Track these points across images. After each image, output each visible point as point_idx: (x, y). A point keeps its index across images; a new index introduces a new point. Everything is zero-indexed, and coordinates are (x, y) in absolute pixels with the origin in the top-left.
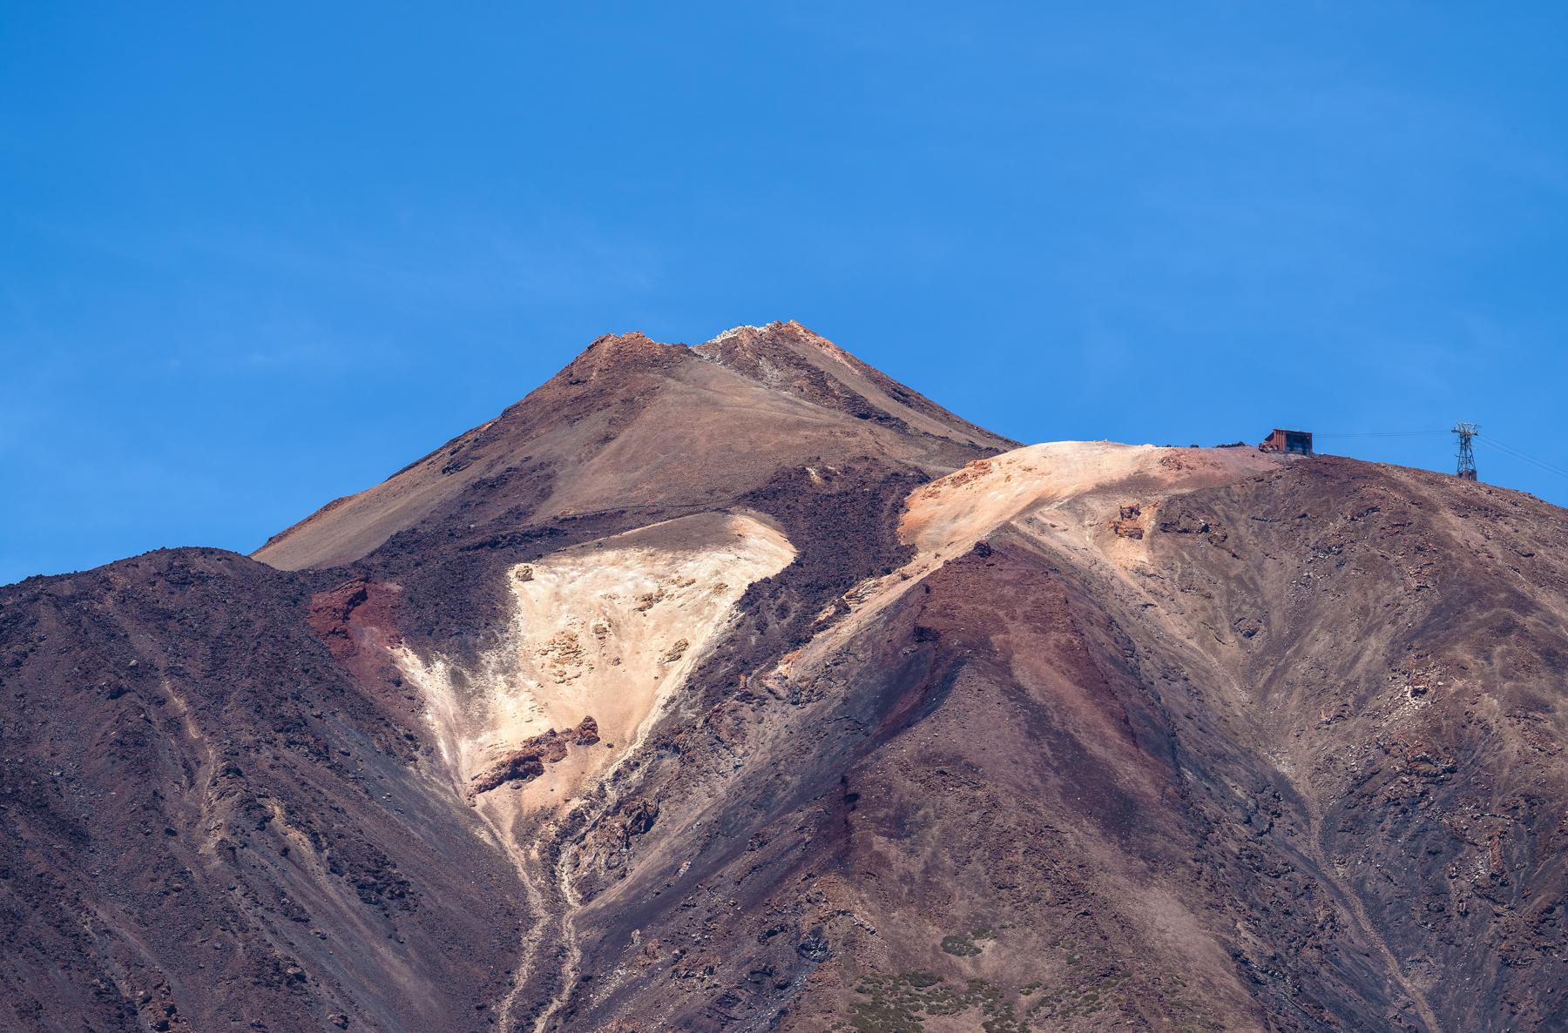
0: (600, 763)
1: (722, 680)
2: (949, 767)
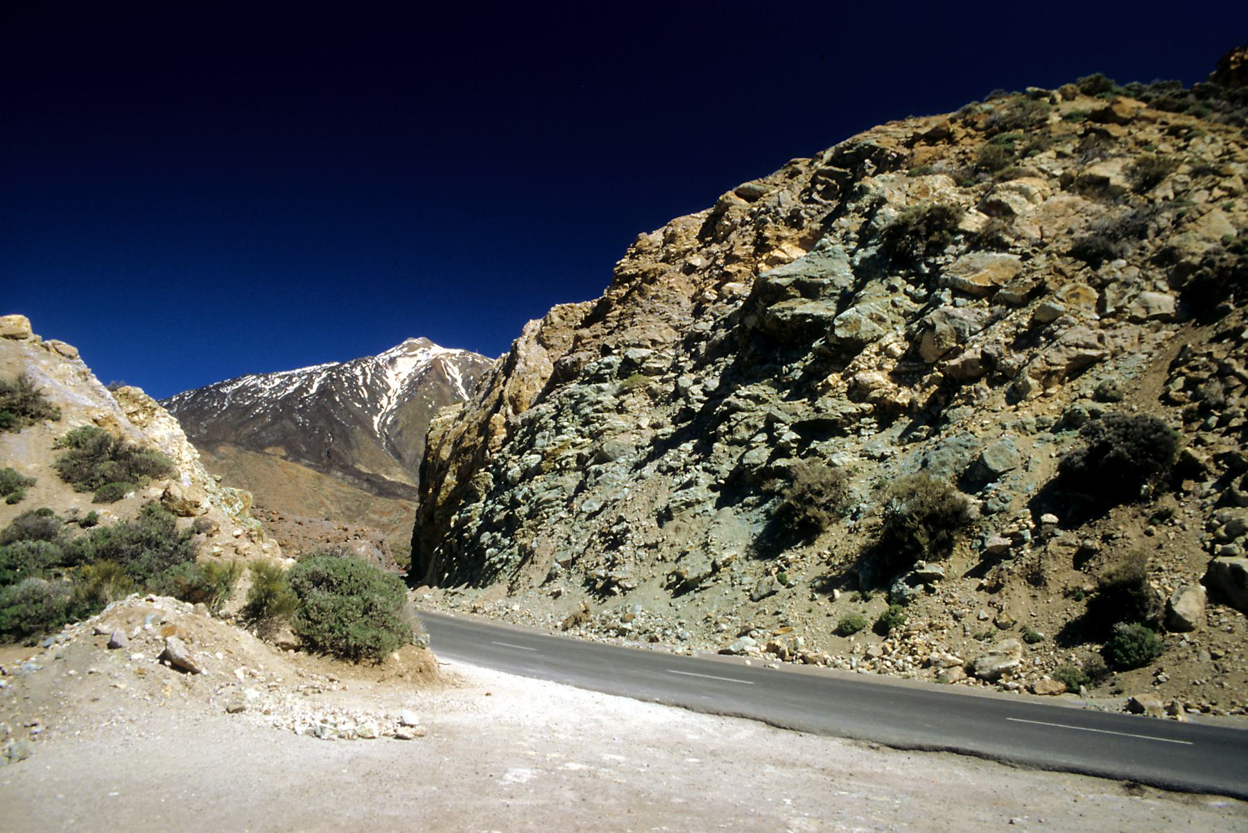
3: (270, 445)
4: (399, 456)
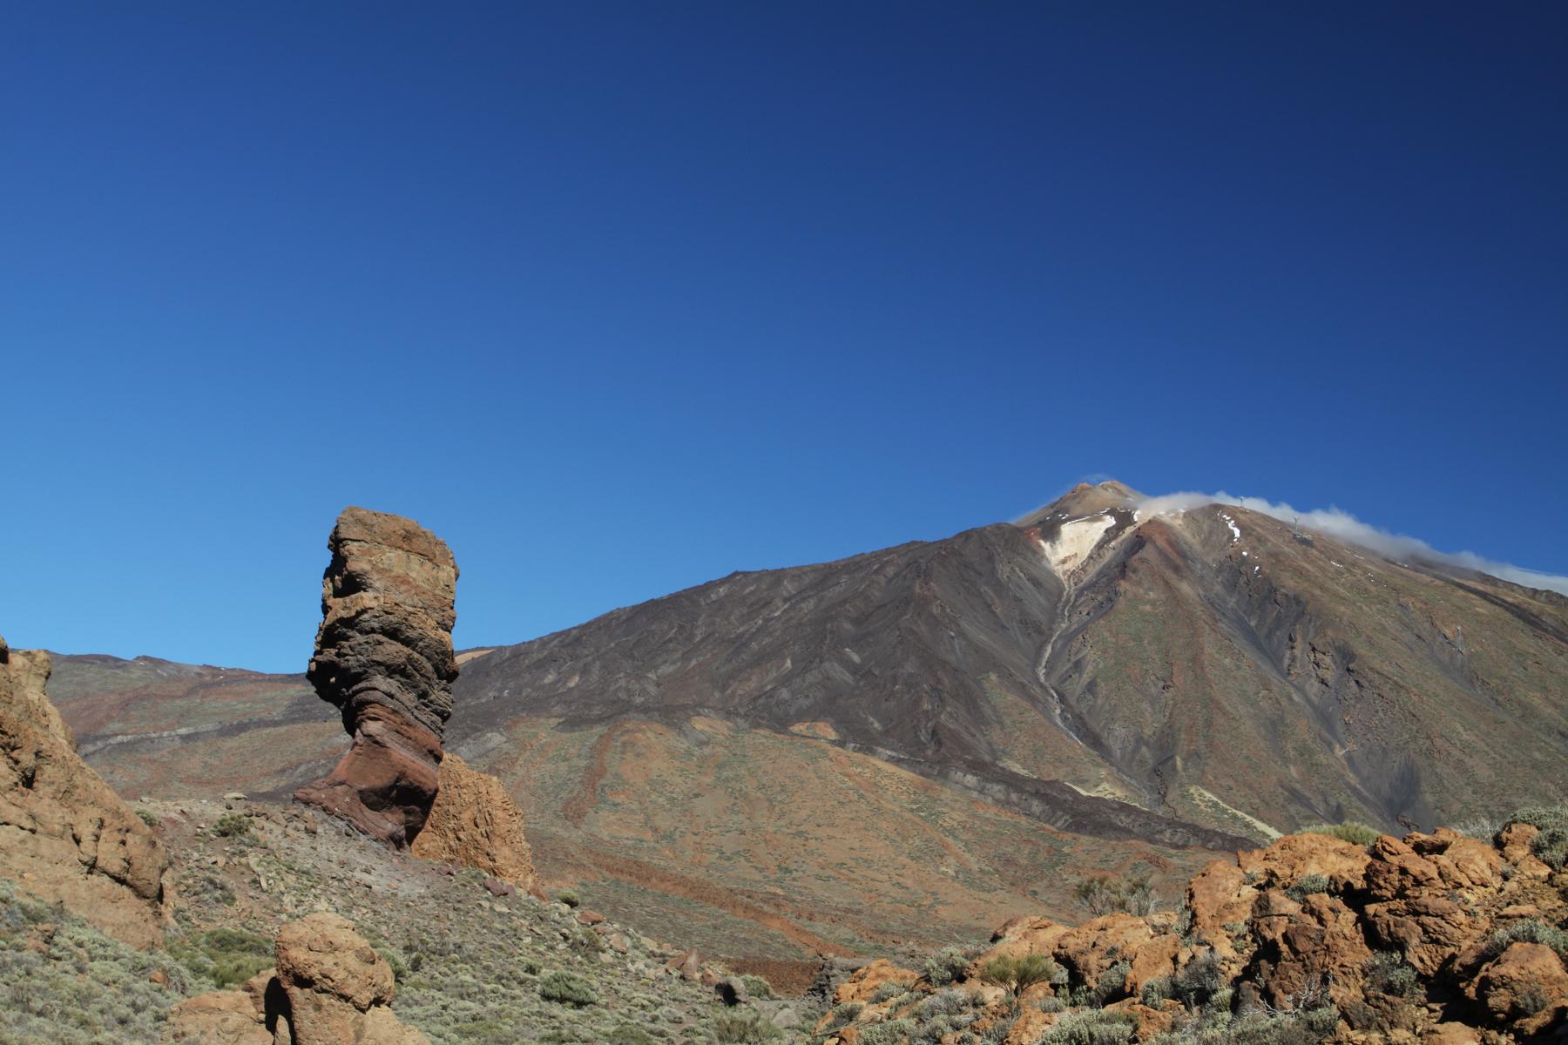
0: (1079, 561)
1: (1100, 546)
2: (1143, 560)
3: (800, 716)
4: (1095, 741)
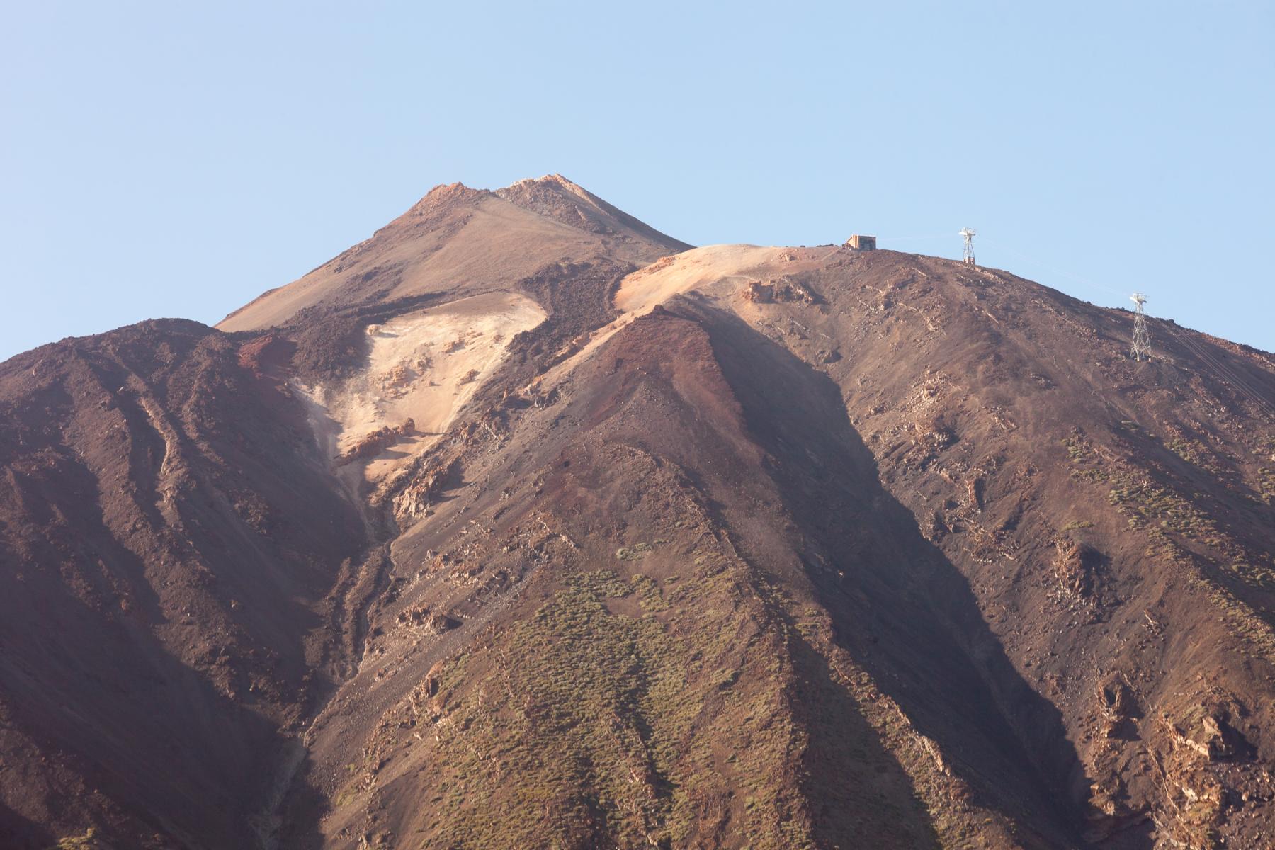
0: (418, 449)
